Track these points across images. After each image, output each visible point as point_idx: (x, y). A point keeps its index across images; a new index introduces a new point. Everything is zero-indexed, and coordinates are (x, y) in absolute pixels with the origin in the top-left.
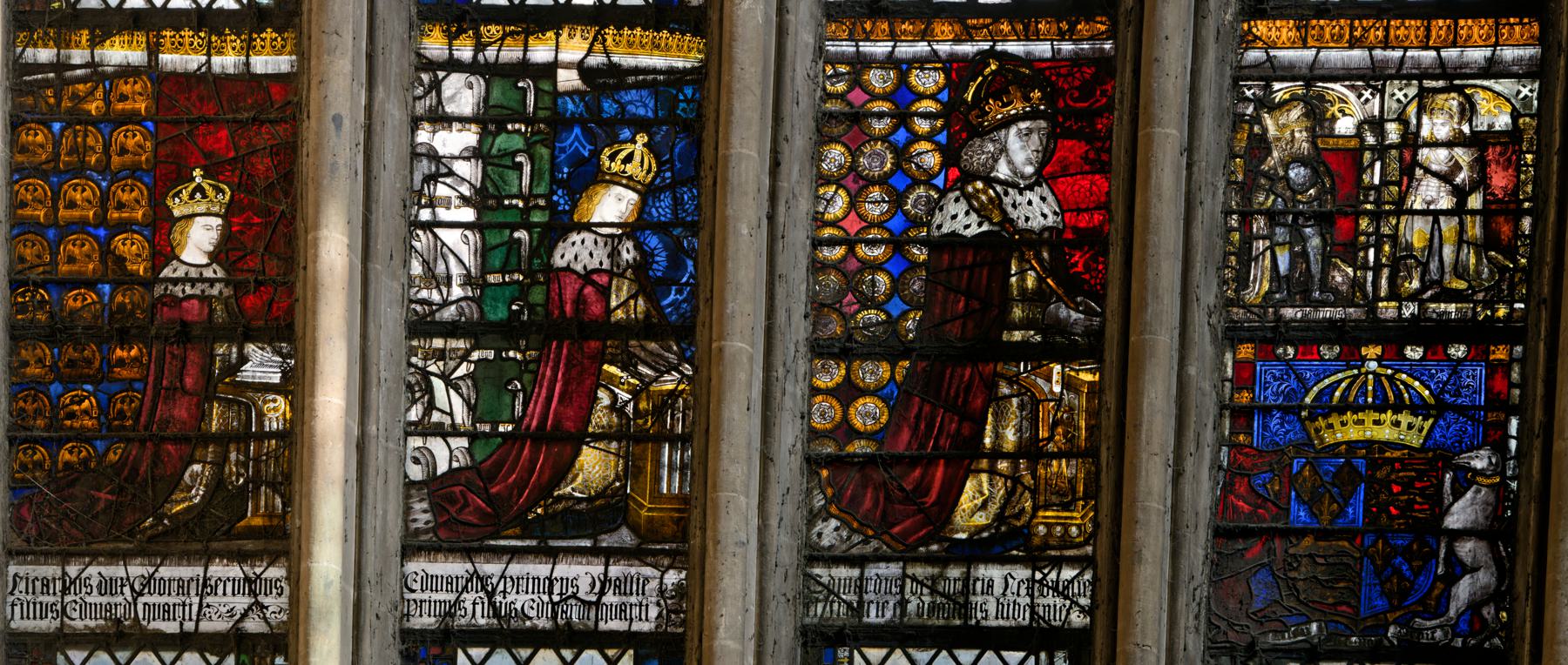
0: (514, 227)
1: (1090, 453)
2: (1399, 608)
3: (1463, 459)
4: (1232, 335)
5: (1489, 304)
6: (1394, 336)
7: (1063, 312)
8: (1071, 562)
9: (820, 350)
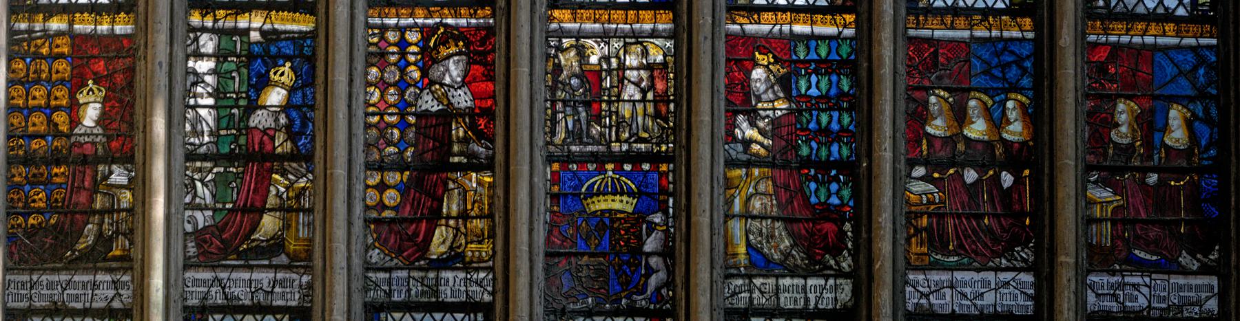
1: (491, 216)
2: (626, 290)
3: (650, 218)
4: (550, 159)
5: (658, 145)
6: (619, 159)
9: (369, 166)
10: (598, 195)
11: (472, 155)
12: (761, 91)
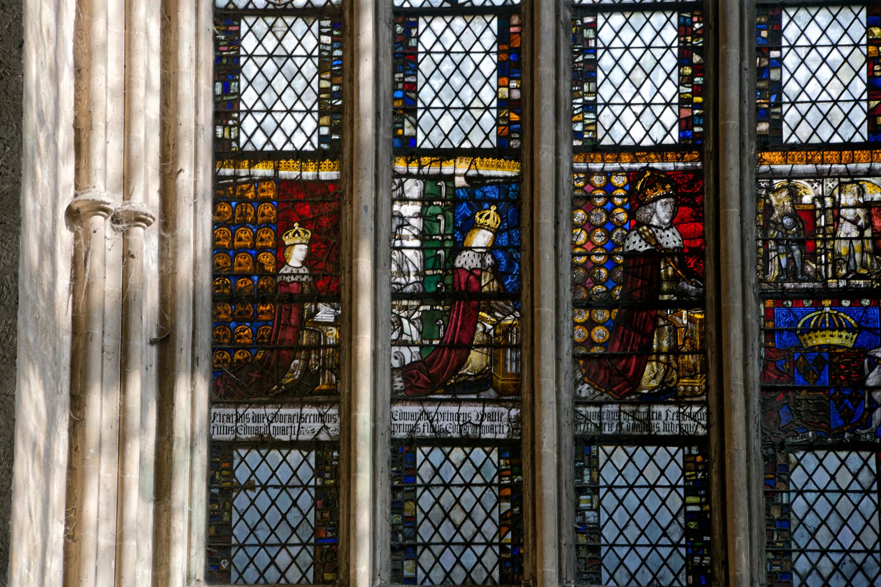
1: (703, 352)
4: (763, 296)
6: (837, 295)
7: (686, 286)
8: (697, 403)
9: (577, 305)
10: (815, 331)
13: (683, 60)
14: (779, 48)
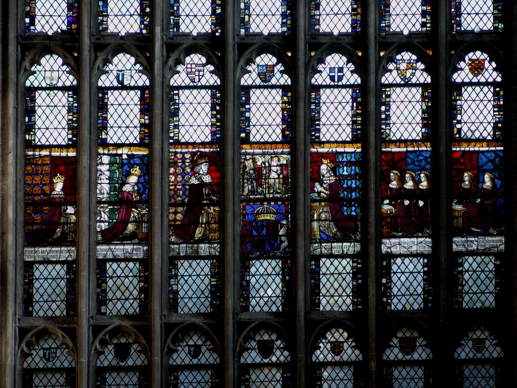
0: (116, 184)
5: (284, 194)
6: (269, 200)
8: (216, 243)
9: (171, 205)
11: (212, 200)
12: (325, 173)
13: (213, 108)
14: (249, 104)
